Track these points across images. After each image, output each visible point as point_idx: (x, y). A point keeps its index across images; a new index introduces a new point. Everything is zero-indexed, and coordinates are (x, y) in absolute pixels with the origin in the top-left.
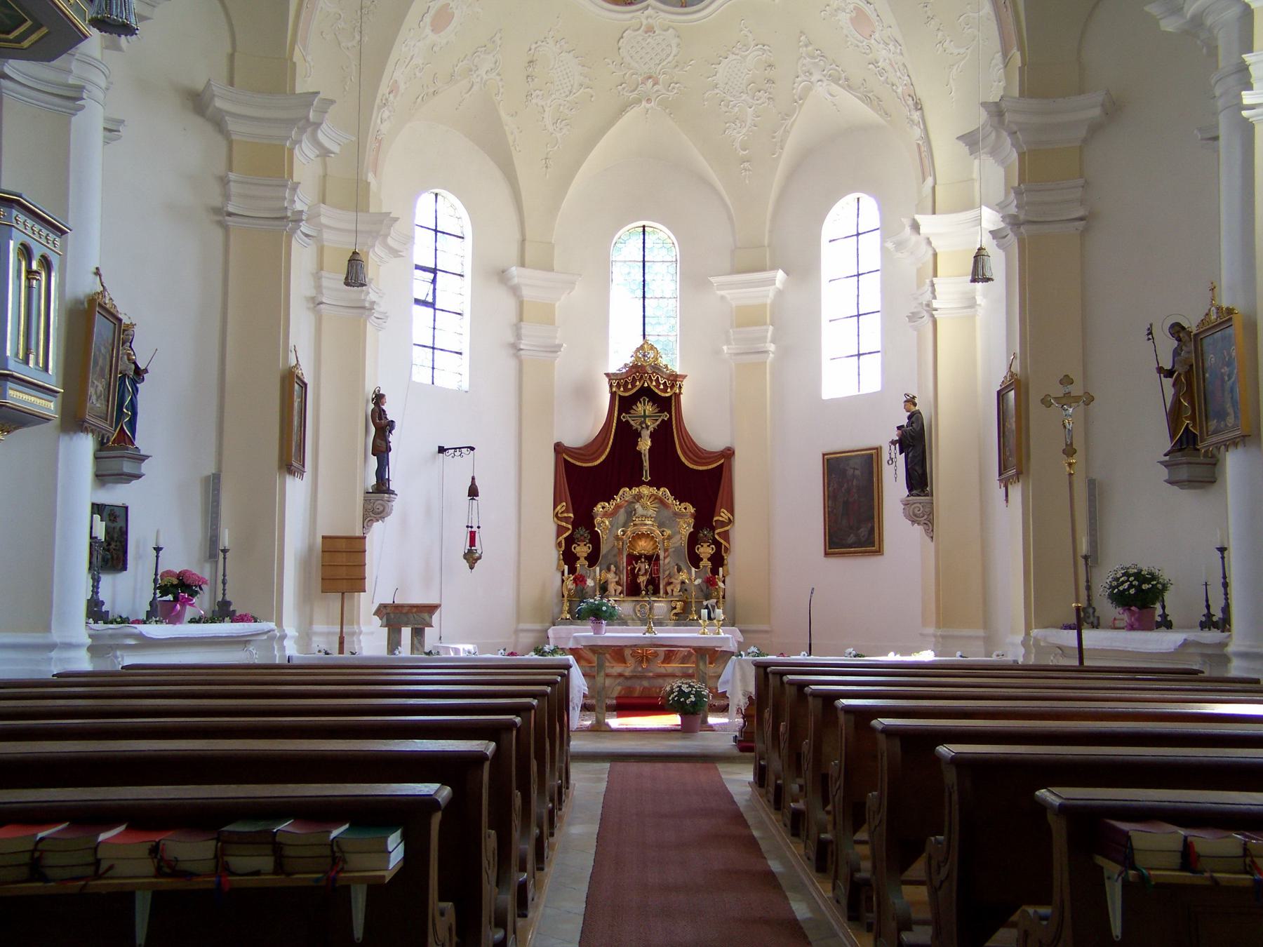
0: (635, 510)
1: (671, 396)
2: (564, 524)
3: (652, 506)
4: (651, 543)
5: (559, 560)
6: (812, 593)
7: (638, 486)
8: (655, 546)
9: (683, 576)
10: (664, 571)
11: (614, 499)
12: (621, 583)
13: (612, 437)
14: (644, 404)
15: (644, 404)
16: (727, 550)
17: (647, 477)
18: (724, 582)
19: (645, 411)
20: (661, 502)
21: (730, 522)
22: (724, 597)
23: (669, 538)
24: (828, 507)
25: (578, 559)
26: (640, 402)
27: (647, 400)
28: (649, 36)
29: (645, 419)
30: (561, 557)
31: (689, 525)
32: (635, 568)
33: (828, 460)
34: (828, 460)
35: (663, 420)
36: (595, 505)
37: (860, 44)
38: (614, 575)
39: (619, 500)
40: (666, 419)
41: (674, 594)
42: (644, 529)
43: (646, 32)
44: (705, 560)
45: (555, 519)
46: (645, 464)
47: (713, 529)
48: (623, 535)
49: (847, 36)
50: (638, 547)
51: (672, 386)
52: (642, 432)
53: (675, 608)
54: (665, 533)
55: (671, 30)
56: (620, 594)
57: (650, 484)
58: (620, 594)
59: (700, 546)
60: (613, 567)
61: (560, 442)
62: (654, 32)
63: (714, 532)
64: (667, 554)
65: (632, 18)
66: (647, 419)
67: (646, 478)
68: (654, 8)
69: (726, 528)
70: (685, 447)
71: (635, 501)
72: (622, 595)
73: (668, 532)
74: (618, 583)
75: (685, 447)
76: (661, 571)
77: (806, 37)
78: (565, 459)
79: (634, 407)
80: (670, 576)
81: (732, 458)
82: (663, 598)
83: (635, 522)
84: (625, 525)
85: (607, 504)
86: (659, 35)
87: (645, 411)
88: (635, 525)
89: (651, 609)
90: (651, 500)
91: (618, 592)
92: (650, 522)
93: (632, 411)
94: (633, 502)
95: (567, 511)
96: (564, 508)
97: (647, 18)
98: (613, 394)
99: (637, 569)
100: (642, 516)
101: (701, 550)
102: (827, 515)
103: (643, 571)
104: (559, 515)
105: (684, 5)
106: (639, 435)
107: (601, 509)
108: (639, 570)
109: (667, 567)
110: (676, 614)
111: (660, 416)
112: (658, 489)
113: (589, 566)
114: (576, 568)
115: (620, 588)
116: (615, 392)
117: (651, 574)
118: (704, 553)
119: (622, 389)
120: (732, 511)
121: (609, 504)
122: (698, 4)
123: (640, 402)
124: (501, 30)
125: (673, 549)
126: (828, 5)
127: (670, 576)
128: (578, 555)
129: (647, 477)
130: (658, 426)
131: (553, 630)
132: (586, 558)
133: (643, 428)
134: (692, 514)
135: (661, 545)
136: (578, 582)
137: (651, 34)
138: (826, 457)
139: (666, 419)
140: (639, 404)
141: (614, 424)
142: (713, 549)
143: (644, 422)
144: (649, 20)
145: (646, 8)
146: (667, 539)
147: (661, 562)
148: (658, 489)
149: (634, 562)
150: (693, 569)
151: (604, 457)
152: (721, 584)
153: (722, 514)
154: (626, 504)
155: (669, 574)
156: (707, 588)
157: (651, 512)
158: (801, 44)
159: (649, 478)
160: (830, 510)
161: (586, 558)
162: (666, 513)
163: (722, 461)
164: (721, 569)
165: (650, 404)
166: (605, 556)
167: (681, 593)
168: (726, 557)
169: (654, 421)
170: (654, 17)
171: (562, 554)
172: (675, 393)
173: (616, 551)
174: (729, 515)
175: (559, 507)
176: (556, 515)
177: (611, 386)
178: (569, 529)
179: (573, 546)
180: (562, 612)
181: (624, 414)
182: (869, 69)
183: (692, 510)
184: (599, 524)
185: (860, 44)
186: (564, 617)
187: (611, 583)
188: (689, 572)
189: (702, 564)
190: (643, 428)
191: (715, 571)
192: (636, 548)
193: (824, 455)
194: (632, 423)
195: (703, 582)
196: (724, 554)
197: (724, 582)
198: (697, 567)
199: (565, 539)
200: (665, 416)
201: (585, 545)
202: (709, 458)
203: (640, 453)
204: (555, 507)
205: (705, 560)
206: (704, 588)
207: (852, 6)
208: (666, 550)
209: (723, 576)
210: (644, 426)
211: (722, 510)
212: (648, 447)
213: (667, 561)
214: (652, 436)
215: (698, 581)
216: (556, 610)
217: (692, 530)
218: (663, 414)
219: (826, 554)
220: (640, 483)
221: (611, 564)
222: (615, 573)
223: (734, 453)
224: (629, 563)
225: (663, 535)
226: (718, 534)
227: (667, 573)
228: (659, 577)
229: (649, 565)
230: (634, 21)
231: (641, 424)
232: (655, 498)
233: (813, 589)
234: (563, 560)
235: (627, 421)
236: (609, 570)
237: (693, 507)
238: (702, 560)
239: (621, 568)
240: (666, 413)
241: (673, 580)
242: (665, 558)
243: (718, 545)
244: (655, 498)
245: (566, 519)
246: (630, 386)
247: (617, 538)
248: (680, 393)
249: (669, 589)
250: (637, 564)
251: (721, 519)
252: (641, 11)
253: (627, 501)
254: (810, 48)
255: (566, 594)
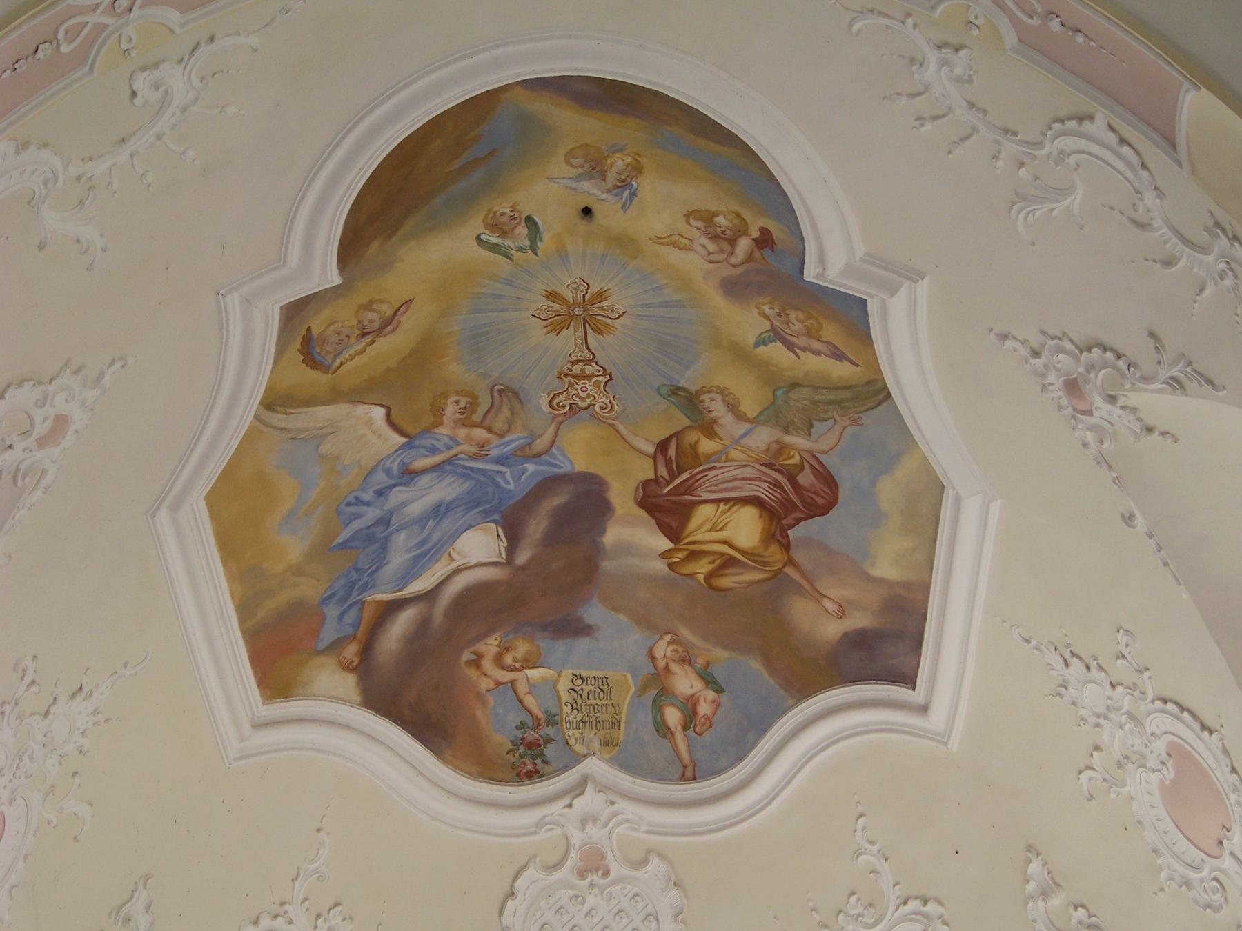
28: (592, 885)
37: (1193, 875)
43: (582, 874)
49: (1155, 851)
55: (655, 864)
62: (606, 873)
65: (540, 824)
68: (602, 788)
77: (1045, 864)
86: (619, 881)
97: (584, 821)
105: (689, 773)
122: (730, 767)
124: (148, 876)
126: (1097, 748)
137: (594, 878)
144: (590, 828)
145: (579, 788)
158: (1031, 887)
170: (603, 818)
185: (1193, 875)
207: (1160, 746)
230: (543, 835)
252: (566, 801)
254: (1056, 901)
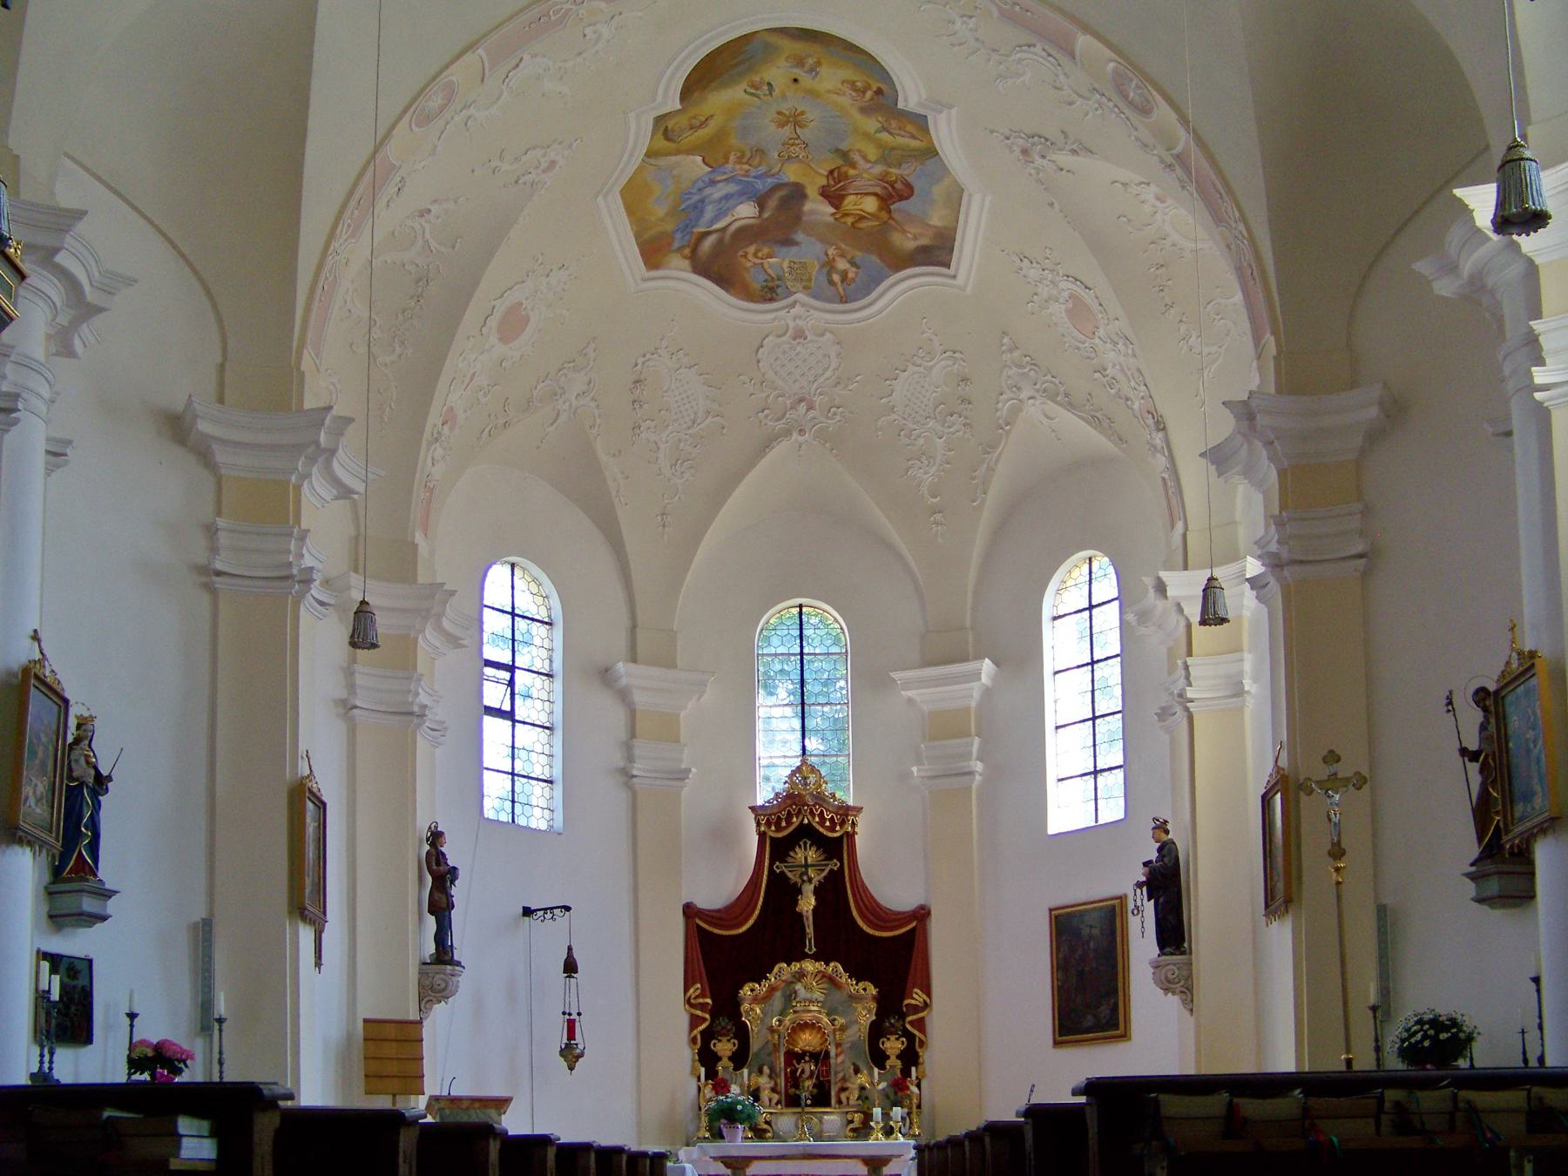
0: (796, 992)
1: (841, 837)
2: (699, 1013)
3: (819, 986)
4: (819, 1036)
5: (694, 1061)
6: (1032, 1091)
7: (798, 960)
8: (823, 1039)
9: (862, 1079)
10: (836, 1073)
11: (767, 978)
12: (779, 1090)
13: (762, 894)
14: (805, 849)
15: (805, 849)
16: (922, 1043)
17: (810, 948)
18: (918, 1086)
19: (806, 859)
20: (831, 980)
21: (926, 1006)
22: (919, 1107)
23: (843, 1029)
24: (1058, 980)
25: (720, 1059)
26: (800, 846)
27: (809, 843)
28: (799, 343)
29: (807, 869)
30: (697, 1057)
31: (869, 1011)
32: (797, 1070)
33: (1056, 917)
34: (1056, 917)
35: (831, 870)
36: (741, 988)
37: (1080, 345)
38: (768, 1079)
39: (773, 979)
40: (835, 869)
41: (851, 1102)
42: (807, 1017)
43: (794, 339)
44: (893, 1058)
45: (687, 1006)
46: (808, 930)
47: (903, 1016)
48: (779, 1025)
49: (1063, 335)
50: (800, 1042)
51: (842, 824)
52: (803, 887)
53: (852, 1122)
54: (836, 1023)
55: (828, 335)
56: (777, 1104)
57: (816, 957)
58: (777, 1104)
59: (885, 1040)
60: (766, 1070)
61: (692, 902)
62: (805, 338)
63: (904, 1021)
64: (839, 1049)
65: (774, 319)
66: (810, 870)
67: (810, 949)
68: (803, 305)
69: (921, 1015)
70: (861, 904)
71: (794, 980)
72: (779, 1106)
73: (840, 1021)
74: (774, 1090)
75: (861, 904)
76: (832, 1073)
77: (1011, 339)
78: (698, 926)
79: (792, 854)
80: (844, 1079)
81: (928, 920)
82: (835, 1108)
83: (795, 1009)
84: (783, 1013)
85: (757, 986)
86: (811, 341)
87: (806, 859)
88: (795, 1012)
89: (821, 1121)
90: (817, 979)
91: (774, 1101)
92: (816, 1008)
93: (789, 859)
94: (792, 982)
95: (703, 995)
96: (699, 991)
97: (795, 319)
98: (762, 835)
99: (799, 1071)
100: (805, 1000)
101: (888, 1044)
102: (1056, 993)
103: (807, 1073)
104: (692, 1001)
105: (844, 299)
106: (799, 891)
107: (749, 993)
108: (803, 1072)
109: (839, 1068)
110: (853, 1130)
111: (827, 865)
112: (827, 964)
113: (736, 1069)
114: (717, 1072)
115: (776, 1097)
116: (764, 832)
117: (818, 1078)
118: (891, 1048)
119: (773, 828)
120: (927, 990)
121: (760, 985)
122: (864, 297)
123: (800, 846)
124: (594, 338)
125: (848, 1045)
126: (1036, 294)
127: (844, 1079)
128: (719, 1054)
129: (810, 948)
130: (825, 878)
131: (686, 1151)
132: (730, 1059)
133: (803, 881)
134: (874, 998)
135: (832, 1037)
136: (719, 1089)
137: (801, 340)
138: (1053, 913)
139: (835, 869)
140: (797, 850)
141: (765, 878)
142: (903, 1043)
143: (806, 873)
144: (798, 321)
145: (793, 305)
146: (840, 1029)
147: (832, 1061)
148: (827, 964)
149: (795, 1062)
150: (876, 1070)
151: (751, 922)
152: (914, 1089)
153: (915, 996)
154: (783, 985)
155: (844, 1076)
156: (896, 1093)
157: (817, 995)
158: (1004, 348)
159: (814, 949)
160: (1060, 984)
161: (730, 1059)
162: (838, 996)
163: (914, 924)
164: (913, 1069)
165: (814, 849)
166: (756, 1055)
167: (860, 1102)
168: (921, 1054)
169: (819, 872)
170: (804, 318)
171: (698, 1054)
172: (847, 833)
173: (770, 1047)
174: (925, 997)
175: (691, 991)
176: (688, 1002)
177: (758, 824)
178: (704, 1020)
179: (713, 1042)
180: (698, 1129)
181: (777, 863)
182: (1095, 380)
183: (873, 990)
184: (747, 1012)
185: (1080, 345)
186: (700, 1135)
187: (764, 1090)
188: (871, 1074)
189: (888, 1064)
190: (803, 881)
191: (906, 1073)
192: (798, 1044)
193: (1051, 910)
194: (790, 875)
195: (888, 1086)
196: (919, 1050)
197: (918, 1086)
198: (882, 1067)
199: (702, 1033)
200: (834, 865)
201: (729, 1041)
202: (894, 920)
203: (800, 915)
204: (686, 990)
205: (893, 1058)
206: (892, 1096)
207: (1066, 294)
208: (838, 1045)
209: (917, 1078)
210: (805, 878)
211: (916, 990)
212: (811, 908)
213: (840, 1059)
214: (817, 892)
215: (883, 1085)
216: (692, 1128)
217: (874, 1018)
218: (831, 862)
219: (1056, 1044)
220: (802, 956)
221: (763, 1065)
222: (770, 1077)
223: (929, 913)
224: (788, 1063)
225: (833, 1025)
226: (911, 1023)
227: (840, 1075)
228: (829, 1081)
229: (816, 1066)
230: (776, 323)
231: (802, 874)
232: (824, 976)
233: (1033, 1086)
234: (700, 1060)
235: (782, 873)
236: (761, 1072)
237: (875, 988)
238: (888, 1057)
239: (778, 1070)
240: (835, 861)
241: (848, 1085)
242: (837, 1055)
243: (911, 1038)
244: (824, 976)
245: (703, 1007)
246: (784, 824)
247: (772, 1030)
248: (854, 833)
249: (843, 1096)
250: (799, 1063)
251: (913, 1002)
252: (787, 310)
253: (783, 981)
254: (1016, 354)
255: (703, 1104)
